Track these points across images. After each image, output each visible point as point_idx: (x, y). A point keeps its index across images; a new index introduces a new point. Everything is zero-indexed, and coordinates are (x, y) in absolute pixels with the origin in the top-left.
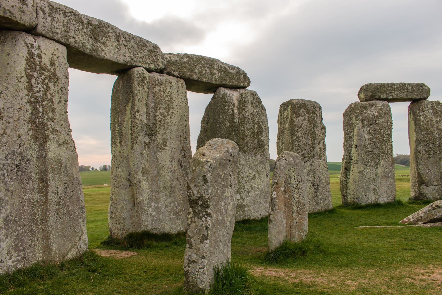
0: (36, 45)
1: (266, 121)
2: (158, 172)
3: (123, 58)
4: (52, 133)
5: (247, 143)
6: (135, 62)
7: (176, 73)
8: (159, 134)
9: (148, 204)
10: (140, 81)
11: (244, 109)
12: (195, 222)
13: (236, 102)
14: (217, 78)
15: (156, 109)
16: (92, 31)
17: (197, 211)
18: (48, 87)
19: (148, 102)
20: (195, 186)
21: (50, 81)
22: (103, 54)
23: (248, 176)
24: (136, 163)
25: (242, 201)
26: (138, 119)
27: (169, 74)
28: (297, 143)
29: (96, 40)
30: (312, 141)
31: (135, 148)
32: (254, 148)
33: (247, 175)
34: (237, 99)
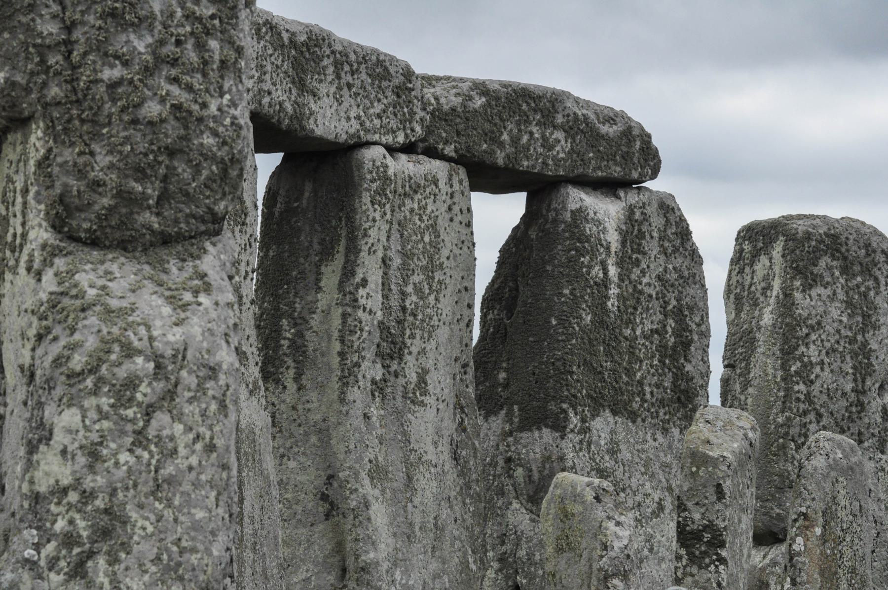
1: (701, 304)
2: (410, 478)
5: (640, 383)
7: (449, 150)
8: (410, 353)
11: (637, 263)
12: (692, 575)
13: (613, 238)
14: (562, 155)
15: (406, 271)
17: (697, 553)
19: (389, 253)
20: (697, 504)
23: (639, 505)
24: (352, 447)
28: (802, 387)
30: (855, 380)
31: (350, 397)
33: (639, 498)
34: (619, 230)
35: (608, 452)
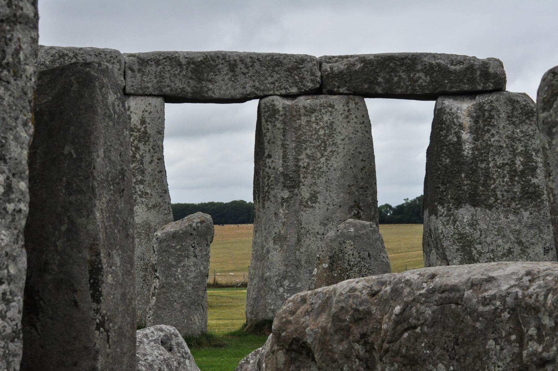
2: (299, 240)
3: (241, 91)
4: (141, 196)
5: (494, 190)
6: (263, 91)
8: (304, 185)
9: (277, 281)
10: (269, 117)
11: (488, 131)
13: (466, 121)
14: (424, 84)
15: (299, 150)
19: (285, 142)
23: (493, 251)
24: (267, 227)
26: (270, 168)
27: (332, 93)
31: (266, 206)
32: (513, 199)
33: (491, 248)
34: (470, 115)
35: (469, 225)
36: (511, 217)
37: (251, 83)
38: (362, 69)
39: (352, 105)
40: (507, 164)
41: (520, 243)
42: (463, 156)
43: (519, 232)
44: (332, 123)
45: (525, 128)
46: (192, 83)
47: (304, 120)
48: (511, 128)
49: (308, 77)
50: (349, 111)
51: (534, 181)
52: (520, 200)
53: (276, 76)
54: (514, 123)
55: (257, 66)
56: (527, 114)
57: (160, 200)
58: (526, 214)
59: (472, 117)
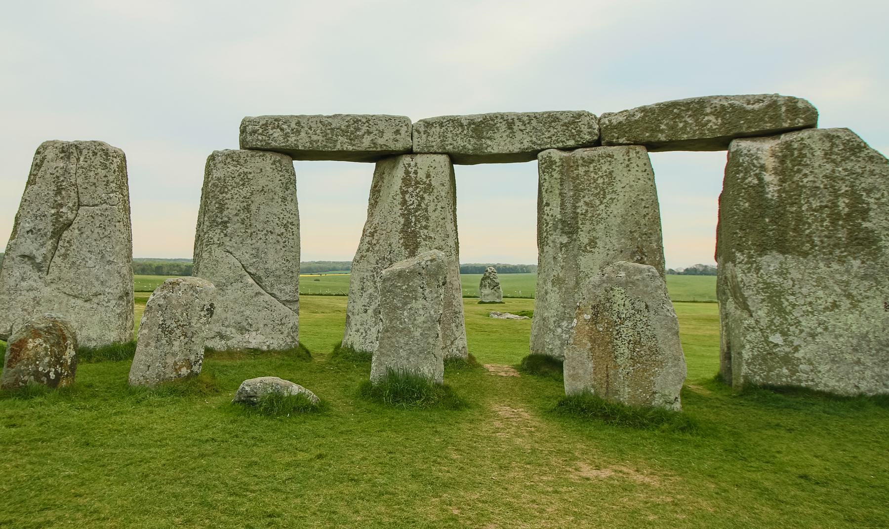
0: (412, 163)
2: (577, 283)
3: (519, 146)
4: (425, 240)
10: (545, 168)
15: (576, 198)
16: (474, 130)
18: (423, 198)
21: (425, 192)
22: (489, 149)
25: (787, 349)
29: (480, 138)
32: (836, 245)
33: (809, 300)
35: (776, 273)
36: (835, 266)
37: (529, 139)
38: (643, 118)
39: (633, 154)
40: (826, 206)
41: (849, 296)
42: (766, 199)
43: (847, 283)
44: (610, 173)
45: (849, 165)
46: (473, 141)
47: (581, 170)
48: (830, 167)
49: (585, 129)
50: (629, 160)
51: (865, 225)
52: (847, 247)
53: (553, 131)
54: (833, 161)
55: (534, 123)
56: (851, 149)
57: (442, 243)
58: (856, 263)
59: (777, 157)
